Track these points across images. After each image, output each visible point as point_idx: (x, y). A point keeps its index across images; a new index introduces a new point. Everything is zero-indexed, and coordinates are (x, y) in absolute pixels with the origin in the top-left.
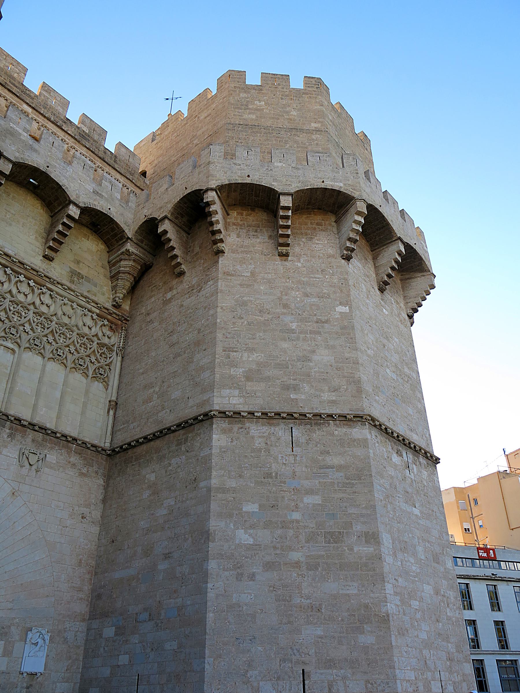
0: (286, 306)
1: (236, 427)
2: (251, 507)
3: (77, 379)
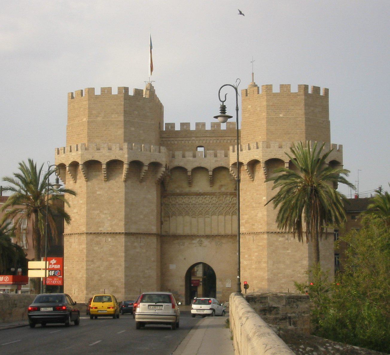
0: (253, 199)
3: (228, 217)
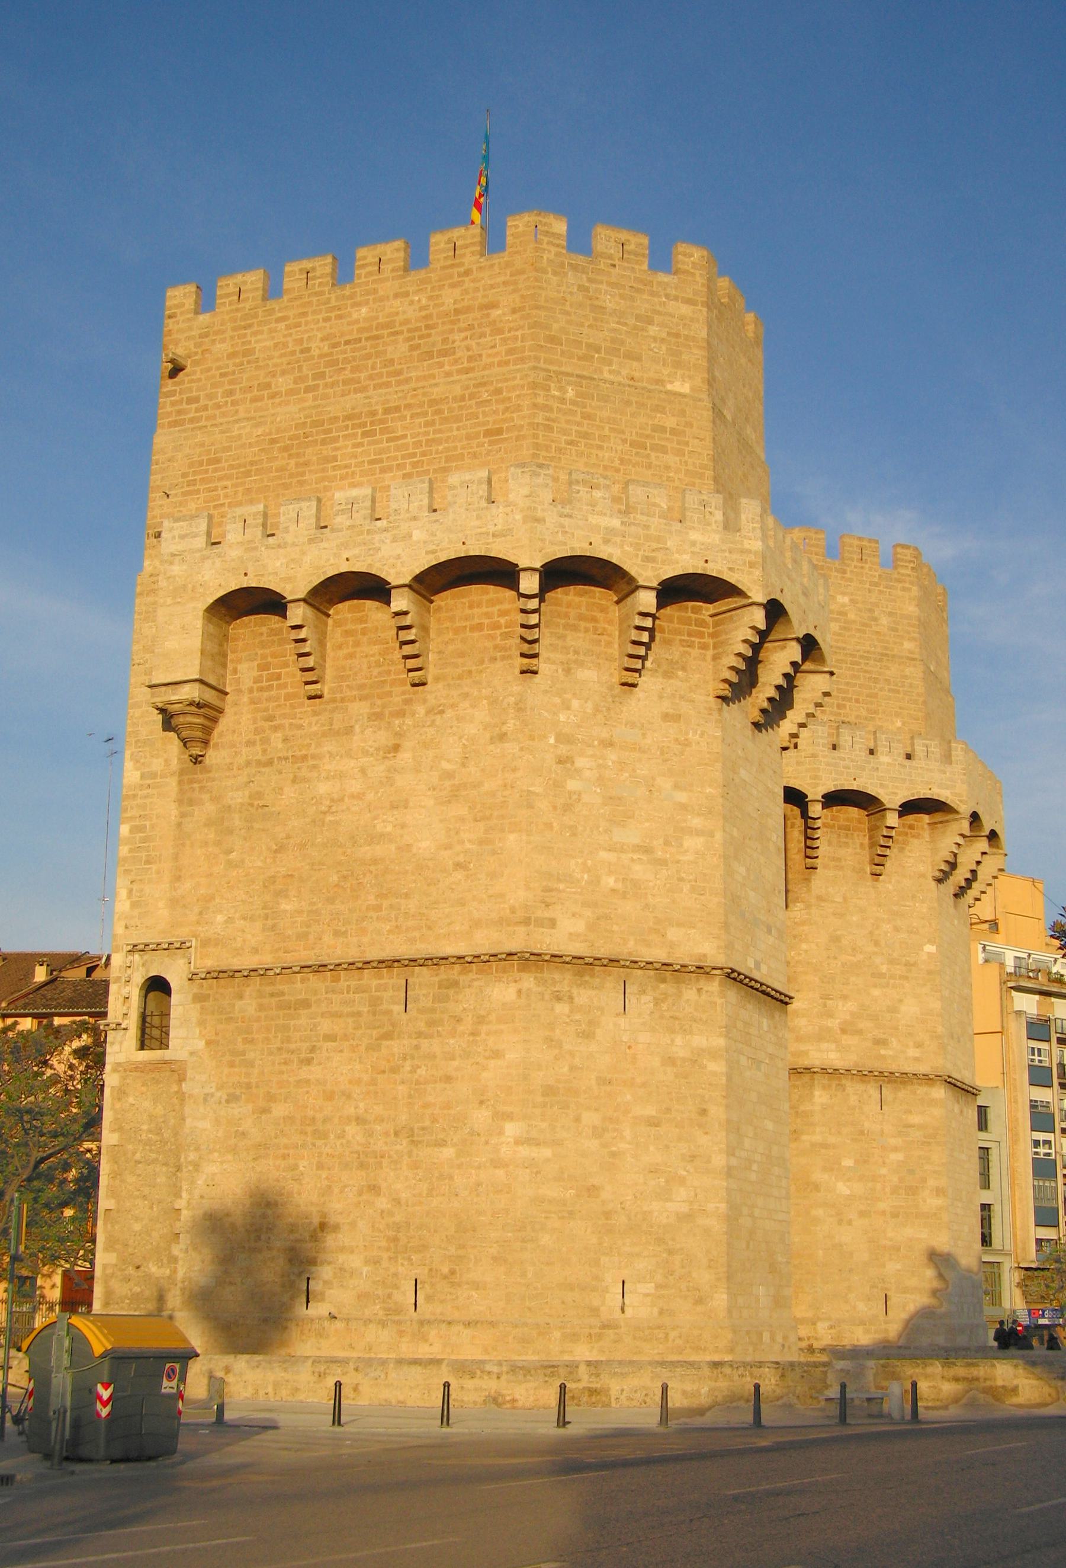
0: (877, 943)
1: (834, 1083)
2: (847, 1162)
